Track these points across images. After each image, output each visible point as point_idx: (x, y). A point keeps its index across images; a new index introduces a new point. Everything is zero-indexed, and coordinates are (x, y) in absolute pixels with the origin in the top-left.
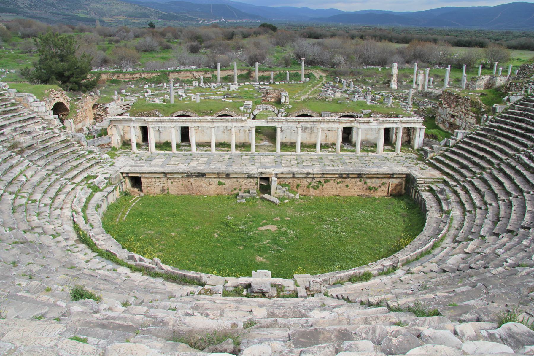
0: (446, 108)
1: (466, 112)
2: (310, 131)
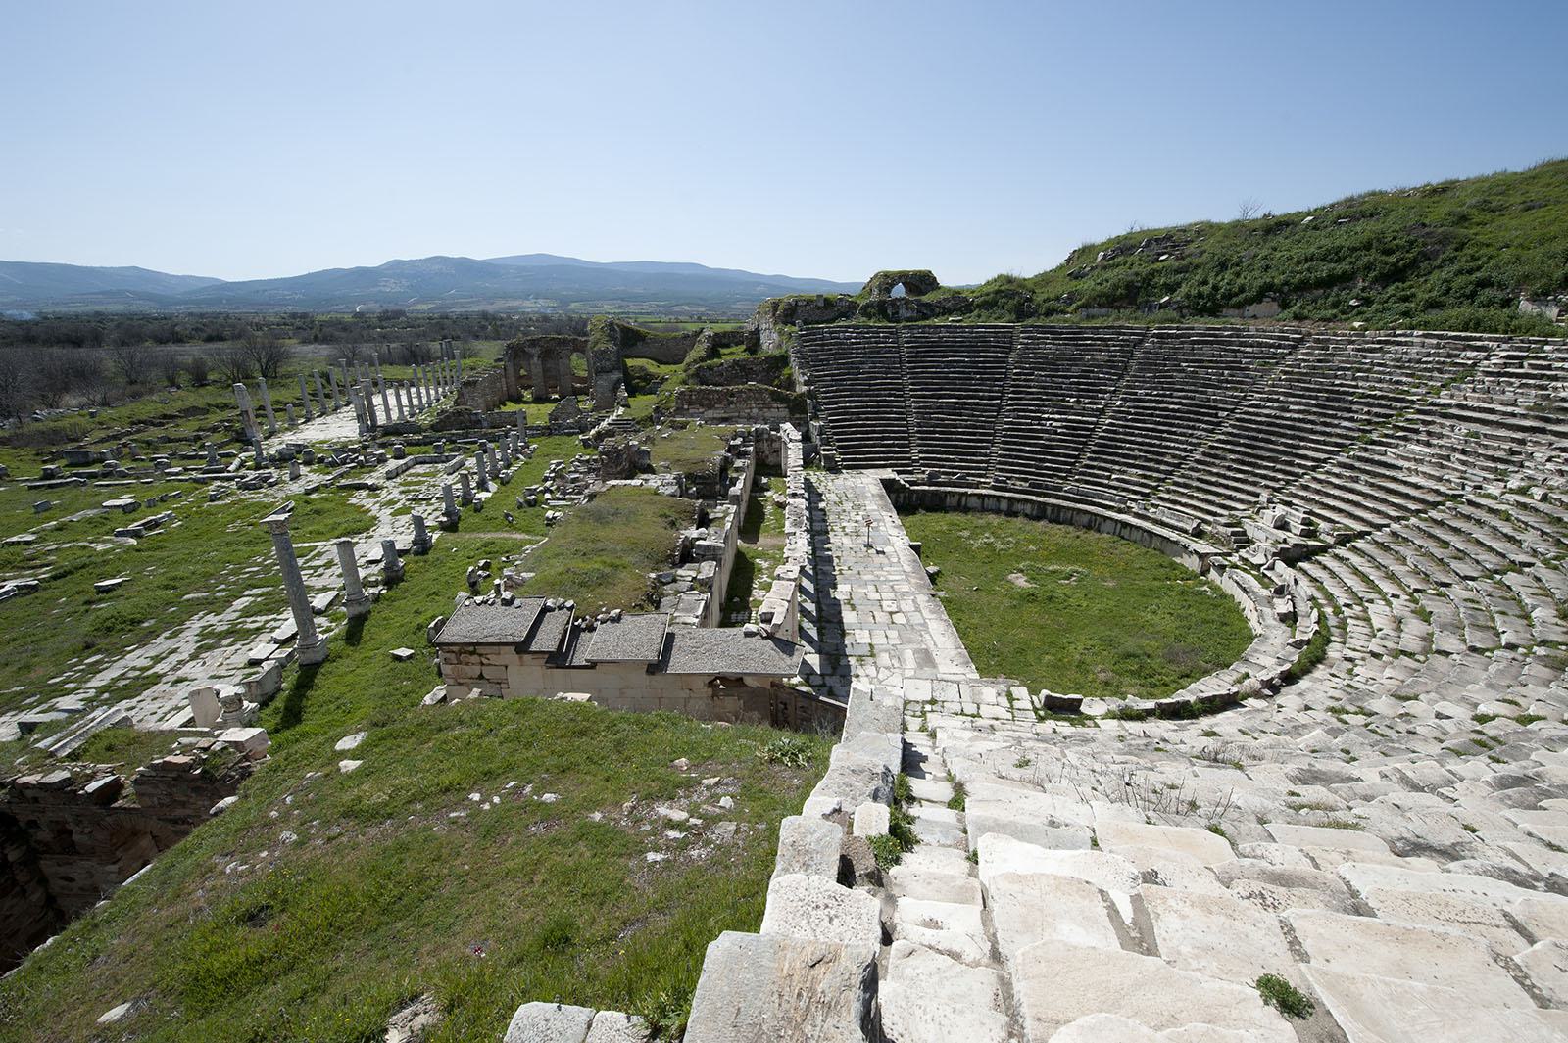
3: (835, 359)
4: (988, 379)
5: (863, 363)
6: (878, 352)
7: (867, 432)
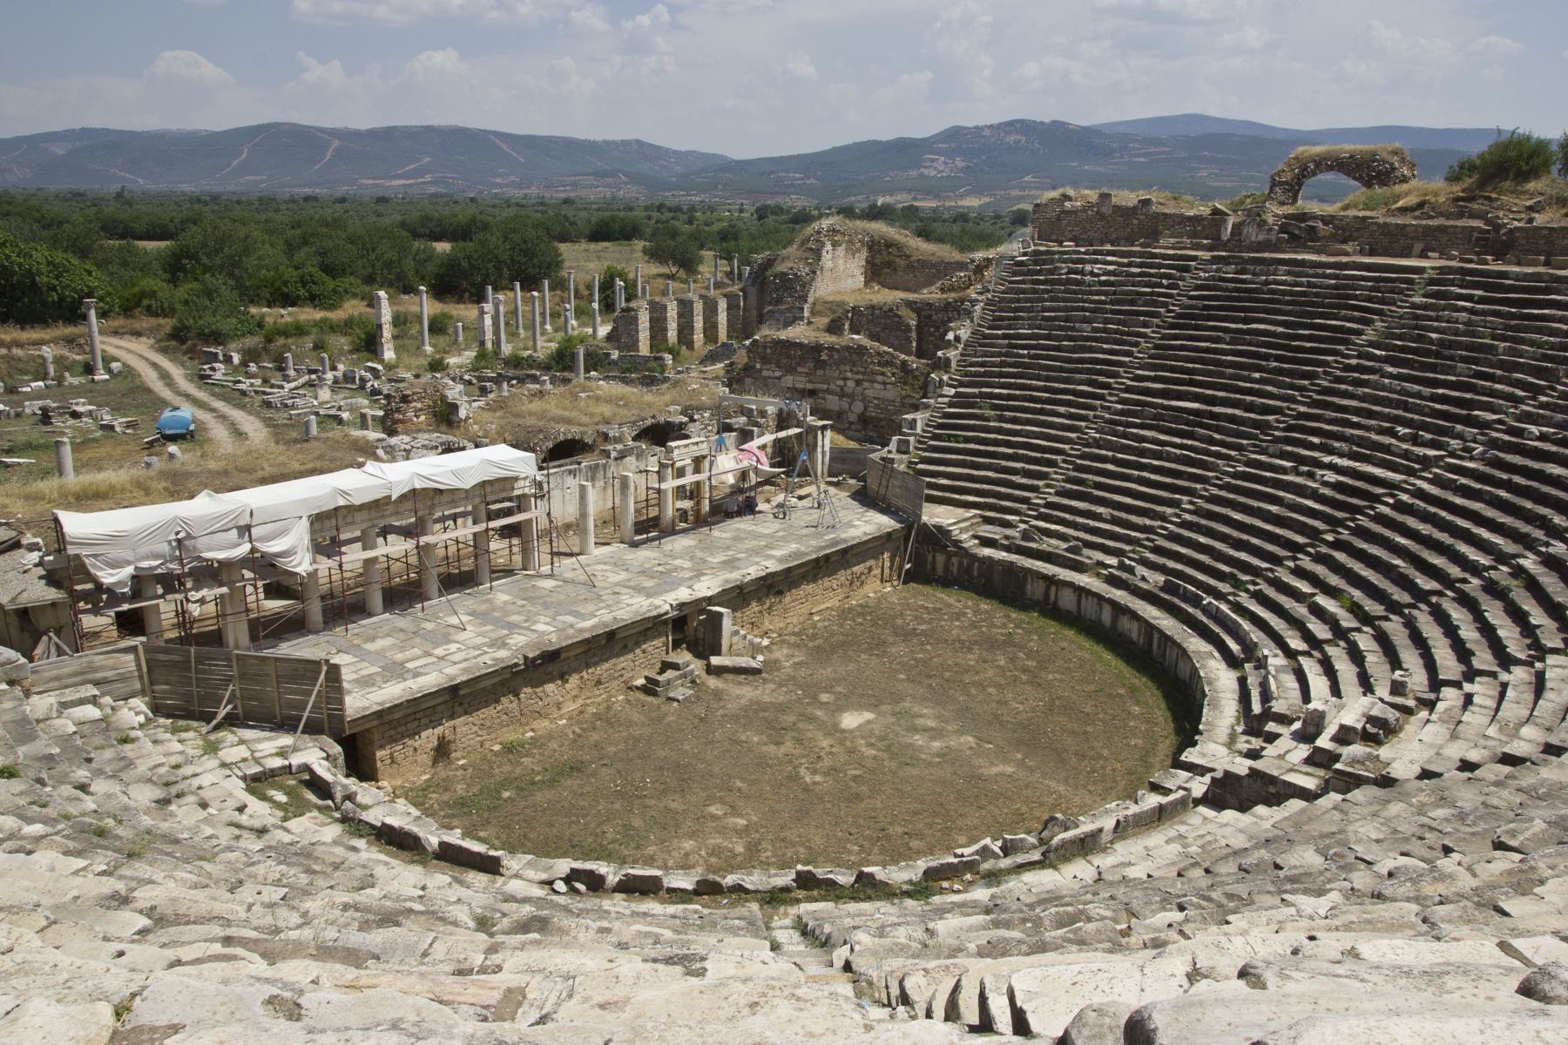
0: (779, 378)
1: (860, 377)
2: (602, 483)
3: (1045, 310)
4: (1290, 373)
5: (1085, 320)
6: (1132, 303)
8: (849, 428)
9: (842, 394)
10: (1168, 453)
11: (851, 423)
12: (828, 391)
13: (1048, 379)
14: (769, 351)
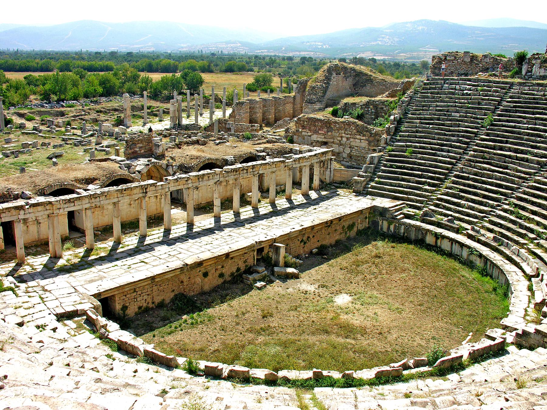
0: (310, 136)
1: (349, 136)
3: (437, 106)
5: (457, 112)
6: (479, 104)
7: (412, 169)
8: (343, 160)
9: (340, 144)
10: (496, 175)
11: (344, 158)
12: (333, 142)
13: (439, 139)
14: (305, 123)
